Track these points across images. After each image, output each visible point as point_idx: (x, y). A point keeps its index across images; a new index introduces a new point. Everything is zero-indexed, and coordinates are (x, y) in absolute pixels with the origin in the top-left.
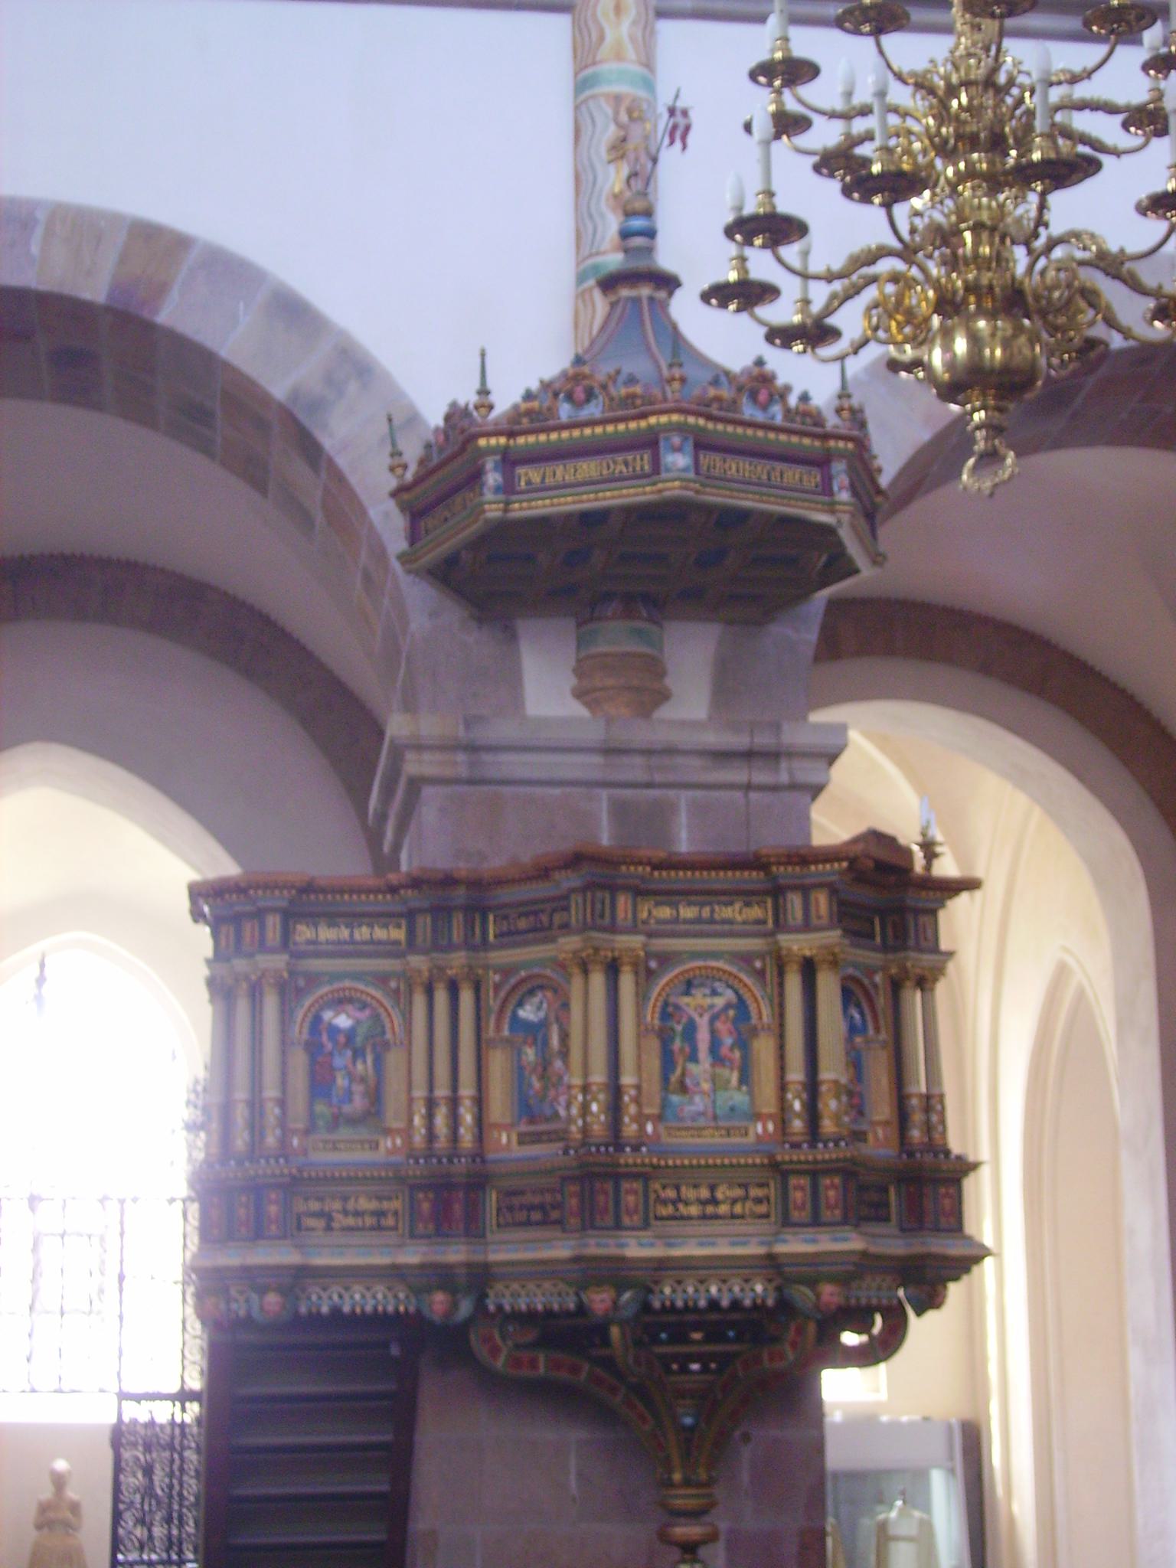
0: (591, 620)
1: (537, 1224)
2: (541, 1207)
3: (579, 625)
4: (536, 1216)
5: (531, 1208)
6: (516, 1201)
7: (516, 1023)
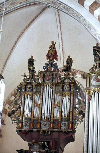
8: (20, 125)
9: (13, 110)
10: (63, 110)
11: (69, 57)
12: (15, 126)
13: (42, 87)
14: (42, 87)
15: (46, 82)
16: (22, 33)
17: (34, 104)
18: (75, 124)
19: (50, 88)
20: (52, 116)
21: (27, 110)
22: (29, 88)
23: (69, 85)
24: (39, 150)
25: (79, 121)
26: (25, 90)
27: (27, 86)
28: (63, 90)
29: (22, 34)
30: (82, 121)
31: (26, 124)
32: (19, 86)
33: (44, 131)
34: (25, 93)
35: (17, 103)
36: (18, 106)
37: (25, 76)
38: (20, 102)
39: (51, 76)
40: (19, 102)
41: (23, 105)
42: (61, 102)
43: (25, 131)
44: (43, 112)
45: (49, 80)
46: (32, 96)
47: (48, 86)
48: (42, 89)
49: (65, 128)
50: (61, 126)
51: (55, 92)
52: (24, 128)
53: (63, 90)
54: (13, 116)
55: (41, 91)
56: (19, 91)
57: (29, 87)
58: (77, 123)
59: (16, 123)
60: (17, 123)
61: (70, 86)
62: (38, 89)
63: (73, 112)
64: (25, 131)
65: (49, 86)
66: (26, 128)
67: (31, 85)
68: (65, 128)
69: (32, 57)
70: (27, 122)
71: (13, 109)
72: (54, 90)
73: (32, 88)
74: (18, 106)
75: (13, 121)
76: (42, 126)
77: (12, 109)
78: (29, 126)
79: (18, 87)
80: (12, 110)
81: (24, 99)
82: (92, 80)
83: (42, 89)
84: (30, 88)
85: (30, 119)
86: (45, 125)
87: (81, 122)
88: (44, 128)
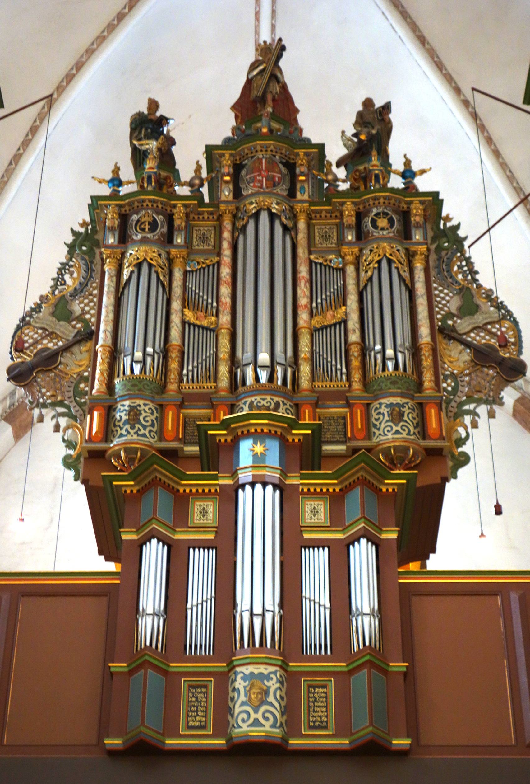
12: (61, 433)
13: (227, 224)
14: (227, 224)
15: (252, 195)
16: (72, 69)
19: (278, 230)
22: (147, 227)
23: (396, 212)
24: (284, 473)
25: (479, 402)
27: (135, 217)
29: (74, 75)
32: (82, 230)
34: (123, 254)
35: (71, 312)
36: (79, 326)
38: (92, 308)
39: (284, 170)
41: (111, 316)
43: (125, 452)
46: (166, 269)
47: (264, 217)
48: (226, 235)
49: (397, 432)
50: (368, 425)
51: (310, 253)
52: (121, 435)
55: (225, 245)
56: (84, 252)
57: (150, 219)
58: (469, 412)
59: (63, 422)
60: (75, 418)
61: (405, 215)
62: (204, 239)
65: (272, 217)
66: (135, 437)
67: (158, 213)
68: (397, 432)
70: (141, 402)
71: (45, 342)
72: (302, 237)
73: (165, 230)
74: (74, 327)
75: (44, 406)
77: (36, 342)
78: (153, 425)
79: (73, 232)
80: (40, 347)
81: (113, 284)
83: (226, 235)
84: (153, 226)
87: (495, 407)
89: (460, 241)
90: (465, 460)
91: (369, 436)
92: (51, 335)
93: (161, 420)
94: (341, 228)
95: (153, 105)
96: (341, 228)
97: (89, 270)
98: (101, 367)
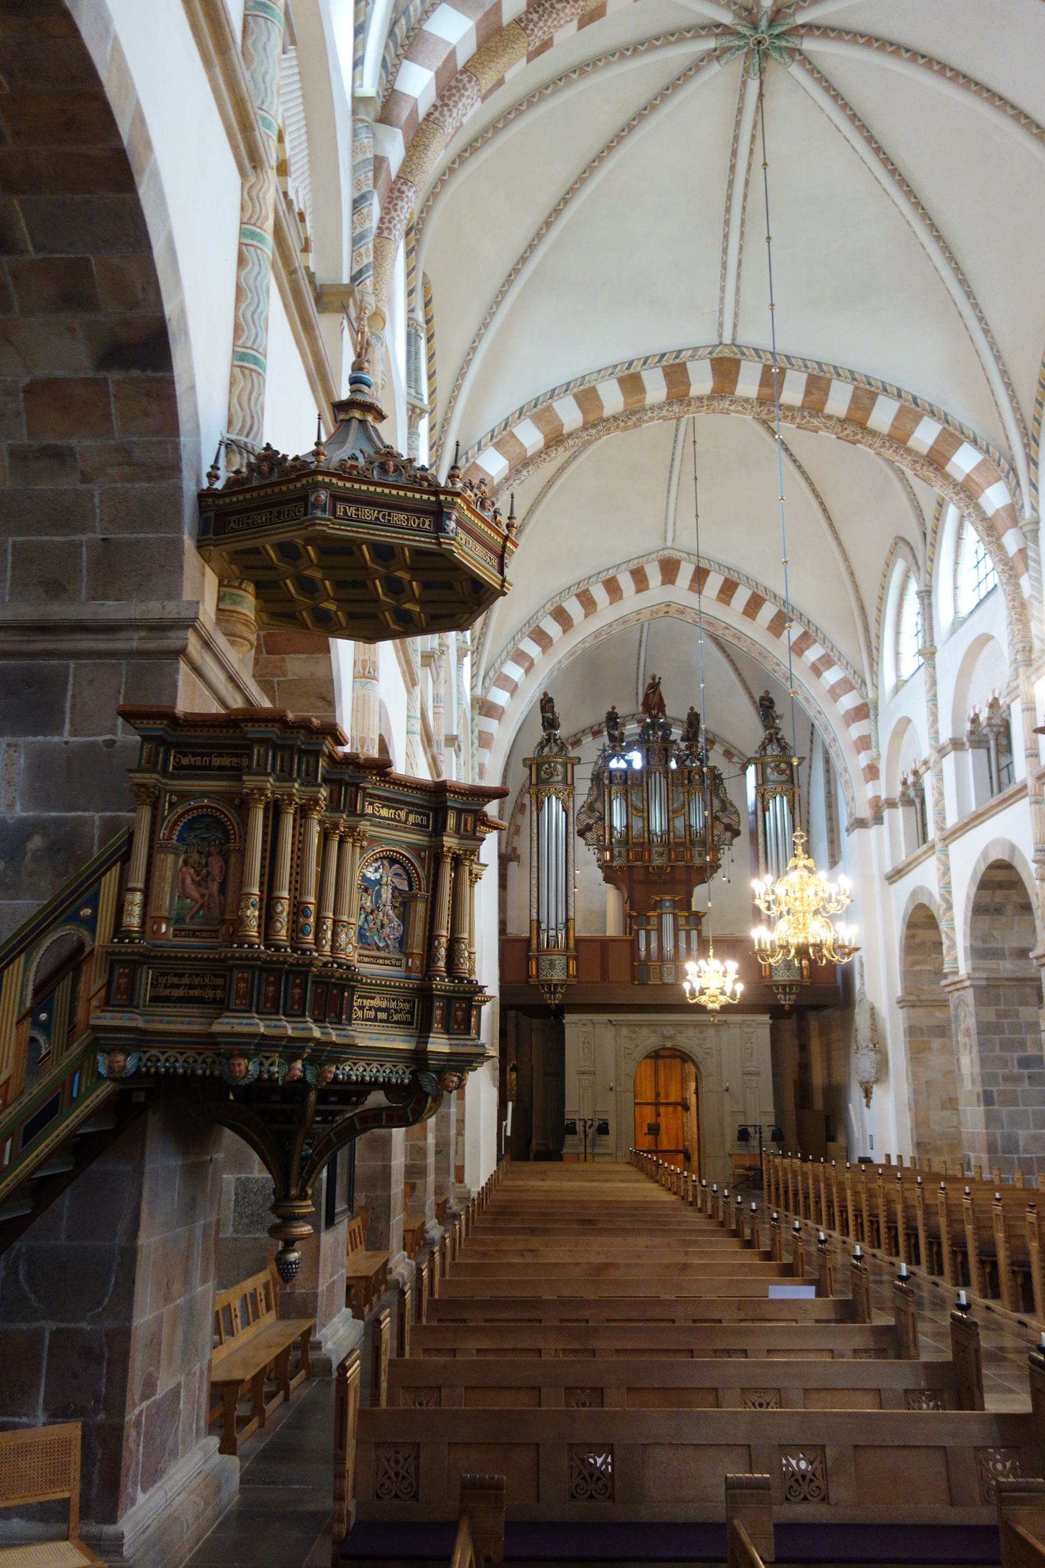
0: (239, 588)
1: (381, 1021)
2: (386, 1010)
3: (220, 585)
4: (382, 1015)
5: (378, 1009)
6: (367, 1003)
7: (364, 878)
8: (608, 855)
9: (588, 824)
10: (693, 822)
11: (692, 709)
17: (630, 809)
18: (718, 850)
20: (672, 835)
21: (617, 822)
26: (611, 782)
28: (690, 781)
30: (731, 844)
31: (620, 852)
33: (660, 868)
37: (604, 750)
40: (598, 805)
42: (687, 807)
44: (652, 828)
45: (660, 760)
50: (691, 856)
53: (690, 781)
54: (588, 834)
63: (712, 827)
64: (620, 867)
69: (614, 708)
76: (654, 856)
82: (769, 770)
85: (627, 842)
86: (661, 854)
88: (658, 862)
89: (721, 780)
90: (719, 866)
91: (691, 861)
92: (590, 818)
93: (628, 855)
94: (683, 778)
95: (614, 708)
96: (683, 778)
97: (599, 790)
98: (607, 832)
